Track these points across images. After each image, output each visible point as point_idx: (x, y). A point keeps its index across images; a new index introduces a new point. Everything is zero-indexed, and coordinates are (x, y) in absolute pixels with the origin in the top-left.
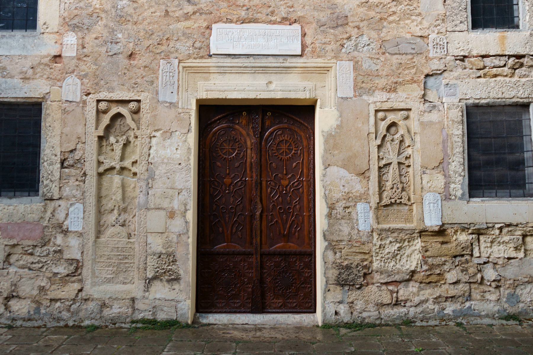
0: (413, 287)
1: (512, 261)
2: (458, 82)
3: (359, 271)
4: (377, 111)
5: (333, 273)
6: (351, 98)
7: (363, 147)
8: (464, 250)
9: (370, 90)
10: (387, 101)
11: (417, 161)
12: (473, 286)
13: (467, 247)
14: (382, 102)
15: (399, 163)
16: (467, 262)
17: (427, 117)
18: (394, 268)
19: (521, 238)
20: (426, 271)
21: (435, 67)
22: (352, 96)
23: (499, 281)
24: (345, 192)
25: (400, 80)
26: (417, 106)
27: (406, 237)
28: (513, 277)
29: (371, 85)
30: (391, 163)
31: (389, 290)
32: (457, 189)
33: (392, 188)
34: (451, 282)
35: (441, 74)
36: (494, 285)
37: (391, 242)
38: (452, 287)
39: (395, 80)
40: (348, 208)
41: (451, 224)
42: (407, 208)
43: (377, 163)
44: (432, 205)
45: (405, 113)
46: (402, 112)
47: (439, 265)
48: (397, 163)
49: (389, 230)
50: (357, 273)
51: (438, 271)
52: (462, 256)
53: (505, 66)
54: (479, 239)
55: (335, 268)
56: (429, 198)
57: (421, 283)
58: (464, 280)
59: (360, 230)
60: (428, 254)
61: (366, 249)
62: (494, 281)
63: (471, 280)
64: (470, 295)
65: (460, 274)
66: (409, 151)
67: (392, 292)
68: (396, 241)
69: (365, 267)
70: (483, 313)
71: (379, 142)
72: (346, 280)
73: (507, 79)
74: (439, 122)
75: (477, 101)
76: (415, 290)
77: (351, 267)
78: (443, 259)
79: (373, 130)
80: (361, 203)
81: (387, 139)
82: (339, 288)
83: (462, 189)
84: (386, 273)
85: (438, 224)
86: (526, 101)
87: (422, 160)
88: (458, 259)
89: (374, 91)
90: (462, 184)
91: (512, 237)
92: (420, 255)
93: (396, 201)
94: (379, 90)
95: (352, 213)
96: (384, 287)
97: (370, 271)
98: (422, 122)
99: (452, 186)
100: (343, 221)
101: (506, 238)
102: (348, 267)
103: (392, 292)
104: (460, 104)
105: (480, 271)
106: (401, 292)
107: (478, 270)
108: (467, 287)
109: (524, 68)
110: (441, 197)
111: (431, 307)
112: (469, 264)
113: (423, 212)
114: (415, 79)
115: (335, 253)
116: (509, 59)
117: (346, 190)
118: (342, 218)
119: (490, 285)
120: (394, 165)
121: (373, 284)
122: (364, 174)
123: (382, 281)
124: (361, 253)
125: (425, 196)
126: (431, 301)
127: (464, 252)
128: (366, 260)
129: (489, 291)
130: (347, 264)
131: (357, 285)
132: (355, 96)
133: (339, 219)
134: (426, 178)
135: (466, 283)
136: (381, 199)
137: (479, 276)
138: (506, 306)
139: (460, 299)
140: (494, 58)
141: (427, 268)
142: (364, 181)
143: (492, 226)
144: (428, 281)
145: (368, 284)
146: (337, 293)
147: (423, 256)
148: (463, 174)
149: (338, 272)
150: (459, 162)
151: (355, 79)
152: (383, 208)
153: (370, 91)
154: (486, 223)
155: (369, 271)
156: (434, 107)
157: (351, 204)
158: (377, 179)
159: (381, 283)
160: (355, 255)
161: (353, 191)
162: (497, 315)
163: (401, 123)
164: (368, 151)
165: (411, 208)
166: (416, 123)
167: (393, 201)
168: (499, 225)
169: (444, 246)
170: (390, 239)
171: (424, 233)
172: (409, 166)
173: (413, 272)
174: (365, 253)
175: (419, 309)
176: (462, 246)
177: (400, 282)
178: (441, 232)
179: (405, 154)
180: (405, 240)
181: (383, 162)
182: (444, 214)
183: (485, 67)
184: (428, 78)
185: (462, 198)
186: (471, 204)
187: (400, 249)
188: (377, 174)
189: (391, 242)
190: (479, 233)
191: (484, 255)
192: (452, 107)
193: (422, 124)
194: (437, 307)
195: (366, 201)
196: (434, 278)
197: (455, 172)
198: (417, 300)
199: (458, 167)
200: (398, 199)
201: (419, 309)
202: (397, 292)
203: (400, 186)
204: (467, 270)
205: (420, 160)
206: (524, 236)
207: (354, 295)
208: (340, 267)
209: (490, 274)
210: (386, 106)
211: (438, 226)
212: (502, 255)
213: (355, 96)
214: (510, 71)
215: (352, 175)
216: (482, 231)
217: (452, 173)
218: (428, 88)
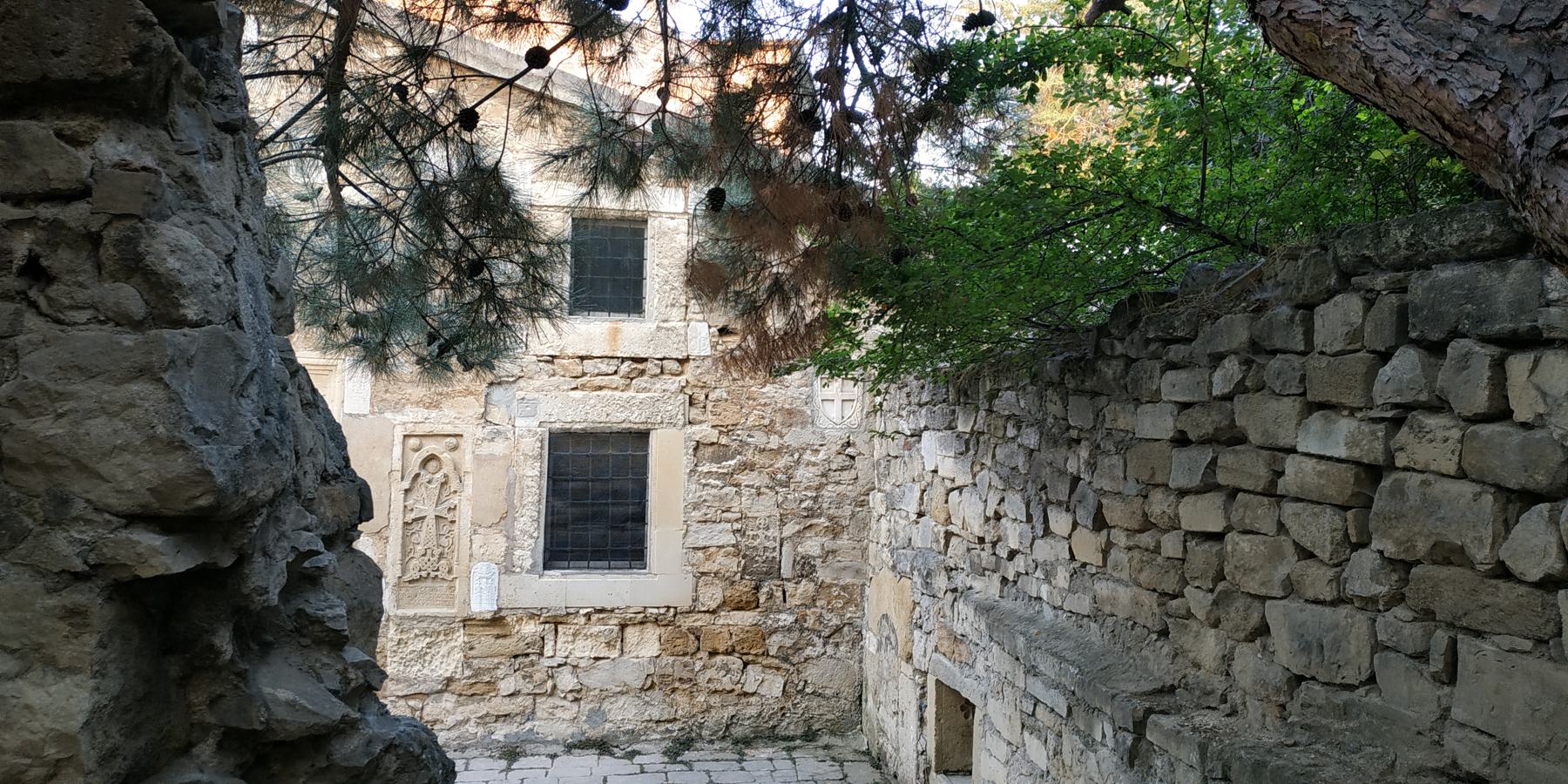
0: (448, 701)
1: (601, 662)
2: (536, 396)
4: (405, 436)
6: (365, 416)
9: (397, 403)
11: (465, 515)
15: (437, 517)
16: (532, 664)
17: (486, 449)
19: (616, 629)
20: (469, 678)
22: (366, 411)
23: (579, 691)
26: (472, 431)
28: (599, 685)
33: (424, 555)
35: (514, 382)
36: (570, 697)
42: (446, 585)
43: (401, 516)
45: (453, 440)
46: (448, 439)
49: (414, 618)
52: (527, 655)
53: (616, 372)
56: (479, 569)
57: (460, 695)
60: (472, 653)
62: (571, 691)
63: (537, 691)
64: (533, 713)
66: (455, 500)
68: (425, 634)
70: (550, 738)
71: (406, 484)
73: (617, 394)
74: (505, 456)
75: (568, 426)
76: (449, 705)
78: (496, 660)
79: (398, 465)
81: (419, 480)
84: (406, 681)
86: (642, 427)
88: (520, 660)
89: (404, 405)
91: (603, 628)
92: (461, 654)
99: (518, 553)
101: (595, 629)
105: (552, 677)
106: (427, 710)
108: (530, 700)
109: (645, 378)
116: (623, 362)
119: (565, 698)
120: (430, 520)
123: (400, 694)
127: (529, 651)
132: (372, 413)
134: (478, 540)
136: (404, 571)
138: (586, 727)
139: (518, 719)
144: (470, 692)
148: (535, 535)
153: (398, 406)
156: (499, 433)
158: (400, 541)
163: (445, 456)
166: (468, 457)
167: (424, 574)
168: (586, 611)
169: (500, 641)
170: (416, 631)
172: (453, 522)
173: (450, 680)
175: (454, 734)
177: (428, 695)
178: (496, 620)
179: (446, 505)
180: (439, 633)
181: (410, 517)
183: (584, 374)
184: (494, 387)
185: (528, 572)
186: (545, 579)
187: (429, 646)
189: (416, 636)
190: (556, 622)
193: (478, 458)
194: (481, 731)
196: (480, 688)
197: (524, 532)
198: (450, 721)
201: (454, 734)
202: (422, 709)
203: (437, 551)
204: (531, 677)
206: (623, 627)
209: (566, 680)
210: (420, 430)
212: (587, 654)
213: (372, 413)
214: (623, 381)
216: (560, 620)
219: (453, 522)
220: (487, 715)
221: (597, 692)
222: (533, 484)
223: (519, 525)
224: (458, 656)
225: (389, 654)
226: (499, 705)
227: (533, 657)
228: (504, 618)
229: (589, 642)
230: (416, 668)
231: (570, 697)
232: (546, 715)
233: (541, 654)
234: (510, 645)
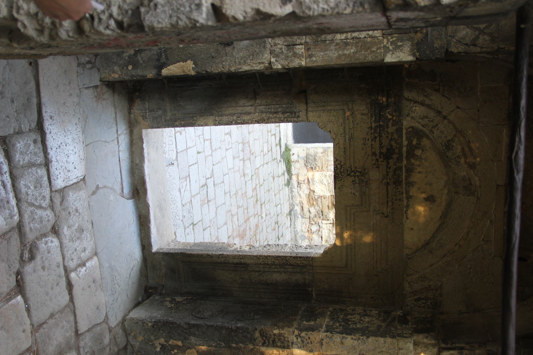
1: (321, 239)
3: (313, 165)
5: (312, 152)
12: (308, 220)
13: (326, 218)
16: (320, 217)
18: (316, 182)
20: (315, 198)
27: (331, 189)
28: (313, 238)
36: (309, 229)
37: (328, 181)
38: (308, 210)
47: (317, 204)
50: (313, 164)
51: (315, 203)
54: (331, 223)
58: (311, 215)
60: (323, 198)
61: (324, 168)
62: (311, 230)
64: (304, 218)
67: (304, 181)
68: (328, 183)
69: (315, 168)
70: (296, 223)
72: (309, 159)
78: (321, 206)
82: (305, 155)
88: (321, 213)
102: (315, 159)
103: (304, 181)
105: (315, 223)
108: (307, 216)
111: (298, 200)
112: (318, 218)
115: (322, 153)
126: (300, 199)
127: (324, 216)
128: (319, 169)
137: (313, 223)
138: (300, 234)
139: (302, 213)
144: (310, 198)
145: (307, 169)
146: (303, 154)
147: (322, 196)
149: (312, 154)
162: (295, 230)
169: (327, 208)
173: (314, 192)
180: (329, 187)
191: (323, 225)
194: (298, 202)
196: (311, 201)
198: (301, 192)
201: (297, 194)
202: (304, 183)
204: (316, 217)
207: (302, 162)
208: (315, 156)
220: (303, 204)
221: (311, 238)
224: (321, 195)
225: (322, 172)
226: (306, 207)
227: (322, 218)
229: (327, 234)
231: (309, 229)
232: (303, 222)
233: (323, 220)
234: (326, 210)
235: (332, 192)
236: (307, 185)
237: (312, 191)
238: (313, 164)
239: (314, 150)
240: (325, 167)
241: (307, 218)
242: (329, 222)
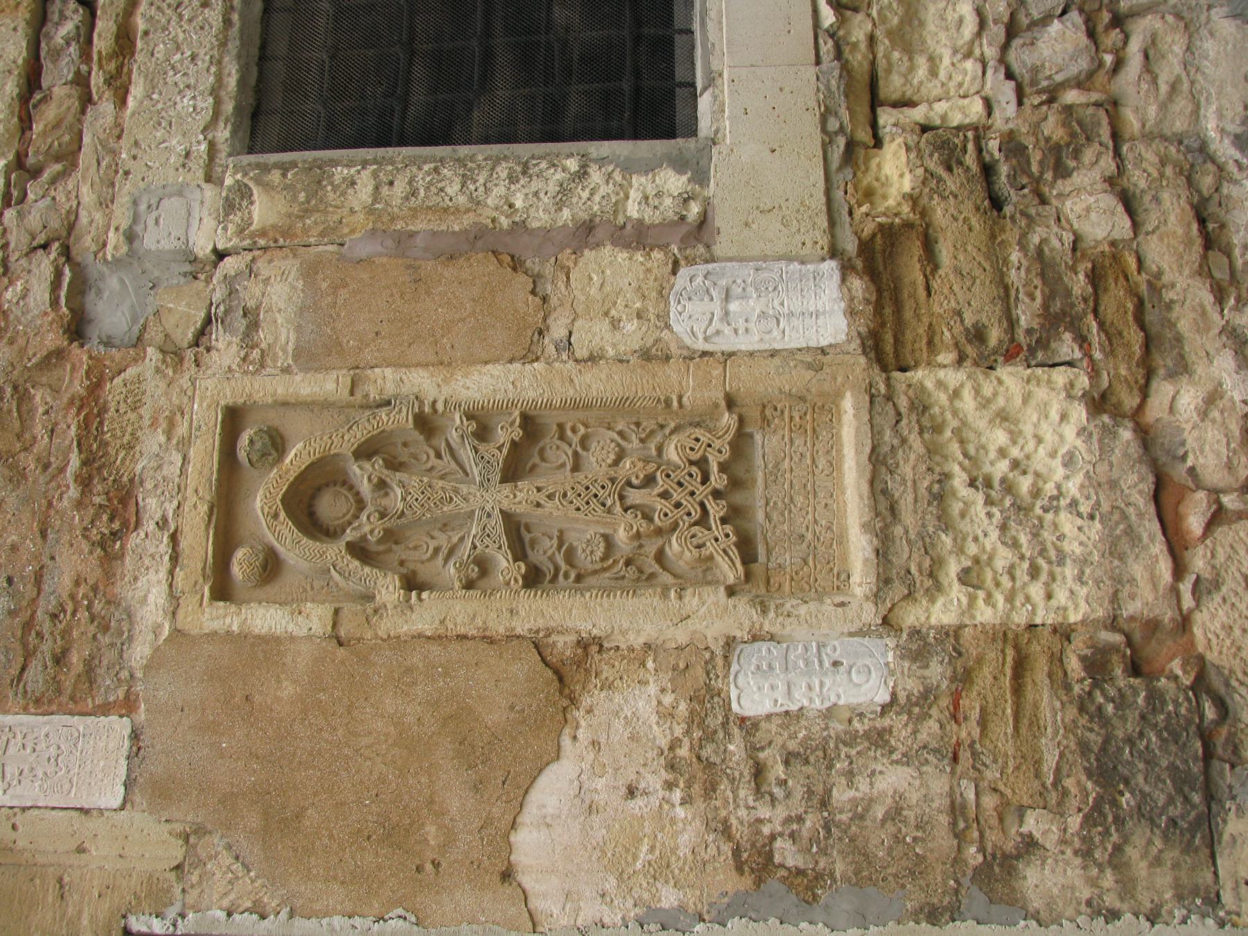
4: (223, 591)
6: (135, 735)
7: (409, 670)
8: (960, 163)
10: (174, 538)
12: (1131, 121)
14: (175, 559)
16: (1013, 147)
20: (1082, 340)
21: (40, 294)
24: (670, 786)
25: (75, 461)
27: (914, 440)
29: (83, 615)
30: (507, 516)
31: (1210, 526)
32: (651, 191)
34: (1127, 223)
38: (1151, 221)
39: (73, 492)
40: (759, 772)
41: (832, 223)
43: (501, 600)
44: (734, 306)
48: (507, 489)
52: (988, 170)
55: (1118, 849)
58: (1108, 164)
59: (887, 698)
60: (995, 335)
62: (1091, 34)
63: (1105, 132)
65: (1076, 179)
69: (1096, 666)
71: (388, 589)
72: (1182, 781)
74: (310, 272)
75: (229, 107)
77: (1103, 749)
80: (734, 694)
83: (649, 168)
85: (837, 276)
87: (496, 361)
90: (629, 168)
92: (1004, 372)
93: (717, 494)
94: (109, 576)
95: (792, 745)
96: (1198, 562)
97: (1117, 638)
98: (297, 355)
100: (841, 795)
104: (228, 181)
107: (1050, 101)
110: (691, 262)
113: (773, 354)
114: (78, 387)
115: (1030, 844)
117: (653, 781)
118: (824, 803)
120: (519, 498)
121: (1184, 623)
122: (565, 671)
123: (1165, 568)
124: (1018, 689)
125: (688, 341)
127: (970, 159)
129: (1146, 57)
130: (1089, 774)
131: (1202, 717)
133: (827, 828)
135: (1117, 153)
139: (1206, 182)
140: (43, 45)
141: (1067, 336)
142: (607, 672)
143: (830, 43)
144: (1135, 337)
149: (1140, 835)
150: (512, 179)
151: (40, 704)
152: (757, 568)
154: (818, 62)
155: (1113, 648)
157: (735, 748)
159: (1179, 571)
160: (1035, 722)
161: (664, 743)
164: (435, 649)
165: (753, 414)
167: (716, 510)
171: (889, 348)
173: (1099, 403)
174: (1021, 667)
176: (941, 171)
181: (503, 562)
182: (780, 248)
188: (563, 599)
192: (236, 218)
195: (720, 662)
199: (536, 184)
200: (705, 480)
205: (496, 369)
211: (843, 280)
213: (128, 706)
215: (566, 741)
217: (566, 213)
218: (136, 330)
219: (528, 421)
220: (1204, 271)
222: (400, 187)
223: (540, 218)
224: (1011, 377)
227: (993, 145)
228: (866, 247)
230: (1067, 523)
232: (1181, 104)
233: (979, 132)
235: (903, 403)
236: (1179, 473)
237: (1118, 414)
238: (1132, 716)
239: (1127, 887)
240: (985, 676)
241: (1148, 137)
242: (918, 114)
